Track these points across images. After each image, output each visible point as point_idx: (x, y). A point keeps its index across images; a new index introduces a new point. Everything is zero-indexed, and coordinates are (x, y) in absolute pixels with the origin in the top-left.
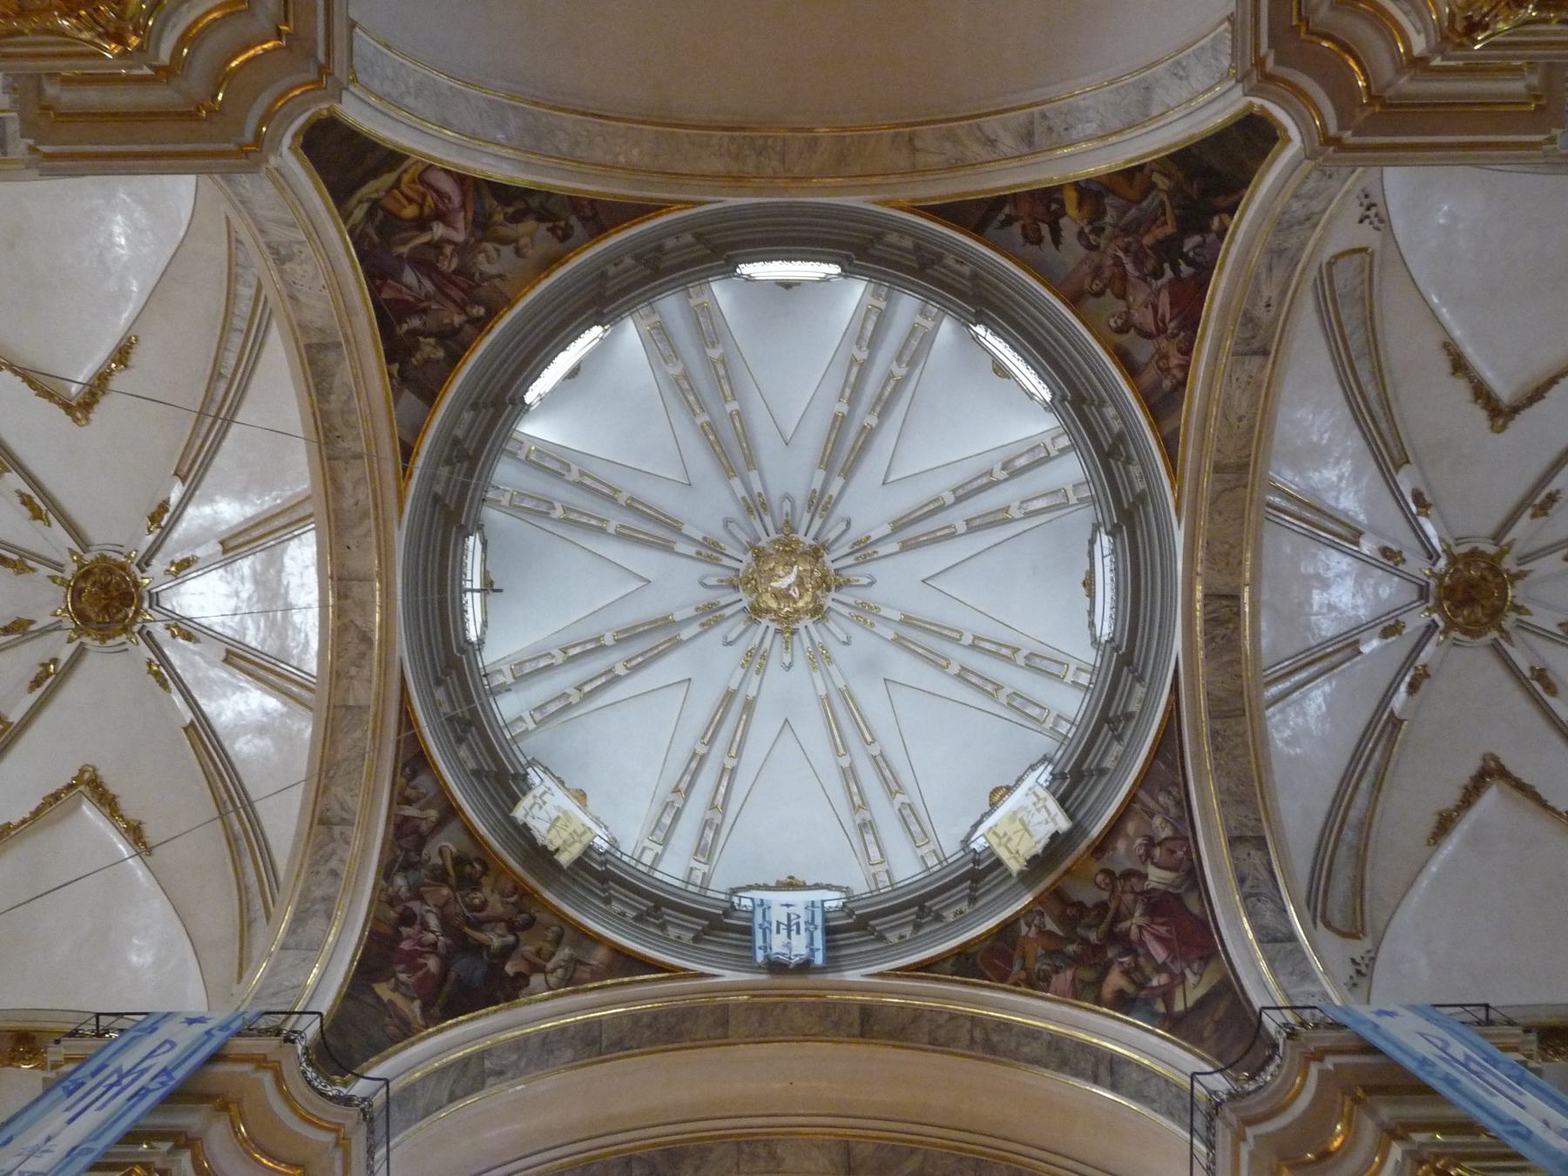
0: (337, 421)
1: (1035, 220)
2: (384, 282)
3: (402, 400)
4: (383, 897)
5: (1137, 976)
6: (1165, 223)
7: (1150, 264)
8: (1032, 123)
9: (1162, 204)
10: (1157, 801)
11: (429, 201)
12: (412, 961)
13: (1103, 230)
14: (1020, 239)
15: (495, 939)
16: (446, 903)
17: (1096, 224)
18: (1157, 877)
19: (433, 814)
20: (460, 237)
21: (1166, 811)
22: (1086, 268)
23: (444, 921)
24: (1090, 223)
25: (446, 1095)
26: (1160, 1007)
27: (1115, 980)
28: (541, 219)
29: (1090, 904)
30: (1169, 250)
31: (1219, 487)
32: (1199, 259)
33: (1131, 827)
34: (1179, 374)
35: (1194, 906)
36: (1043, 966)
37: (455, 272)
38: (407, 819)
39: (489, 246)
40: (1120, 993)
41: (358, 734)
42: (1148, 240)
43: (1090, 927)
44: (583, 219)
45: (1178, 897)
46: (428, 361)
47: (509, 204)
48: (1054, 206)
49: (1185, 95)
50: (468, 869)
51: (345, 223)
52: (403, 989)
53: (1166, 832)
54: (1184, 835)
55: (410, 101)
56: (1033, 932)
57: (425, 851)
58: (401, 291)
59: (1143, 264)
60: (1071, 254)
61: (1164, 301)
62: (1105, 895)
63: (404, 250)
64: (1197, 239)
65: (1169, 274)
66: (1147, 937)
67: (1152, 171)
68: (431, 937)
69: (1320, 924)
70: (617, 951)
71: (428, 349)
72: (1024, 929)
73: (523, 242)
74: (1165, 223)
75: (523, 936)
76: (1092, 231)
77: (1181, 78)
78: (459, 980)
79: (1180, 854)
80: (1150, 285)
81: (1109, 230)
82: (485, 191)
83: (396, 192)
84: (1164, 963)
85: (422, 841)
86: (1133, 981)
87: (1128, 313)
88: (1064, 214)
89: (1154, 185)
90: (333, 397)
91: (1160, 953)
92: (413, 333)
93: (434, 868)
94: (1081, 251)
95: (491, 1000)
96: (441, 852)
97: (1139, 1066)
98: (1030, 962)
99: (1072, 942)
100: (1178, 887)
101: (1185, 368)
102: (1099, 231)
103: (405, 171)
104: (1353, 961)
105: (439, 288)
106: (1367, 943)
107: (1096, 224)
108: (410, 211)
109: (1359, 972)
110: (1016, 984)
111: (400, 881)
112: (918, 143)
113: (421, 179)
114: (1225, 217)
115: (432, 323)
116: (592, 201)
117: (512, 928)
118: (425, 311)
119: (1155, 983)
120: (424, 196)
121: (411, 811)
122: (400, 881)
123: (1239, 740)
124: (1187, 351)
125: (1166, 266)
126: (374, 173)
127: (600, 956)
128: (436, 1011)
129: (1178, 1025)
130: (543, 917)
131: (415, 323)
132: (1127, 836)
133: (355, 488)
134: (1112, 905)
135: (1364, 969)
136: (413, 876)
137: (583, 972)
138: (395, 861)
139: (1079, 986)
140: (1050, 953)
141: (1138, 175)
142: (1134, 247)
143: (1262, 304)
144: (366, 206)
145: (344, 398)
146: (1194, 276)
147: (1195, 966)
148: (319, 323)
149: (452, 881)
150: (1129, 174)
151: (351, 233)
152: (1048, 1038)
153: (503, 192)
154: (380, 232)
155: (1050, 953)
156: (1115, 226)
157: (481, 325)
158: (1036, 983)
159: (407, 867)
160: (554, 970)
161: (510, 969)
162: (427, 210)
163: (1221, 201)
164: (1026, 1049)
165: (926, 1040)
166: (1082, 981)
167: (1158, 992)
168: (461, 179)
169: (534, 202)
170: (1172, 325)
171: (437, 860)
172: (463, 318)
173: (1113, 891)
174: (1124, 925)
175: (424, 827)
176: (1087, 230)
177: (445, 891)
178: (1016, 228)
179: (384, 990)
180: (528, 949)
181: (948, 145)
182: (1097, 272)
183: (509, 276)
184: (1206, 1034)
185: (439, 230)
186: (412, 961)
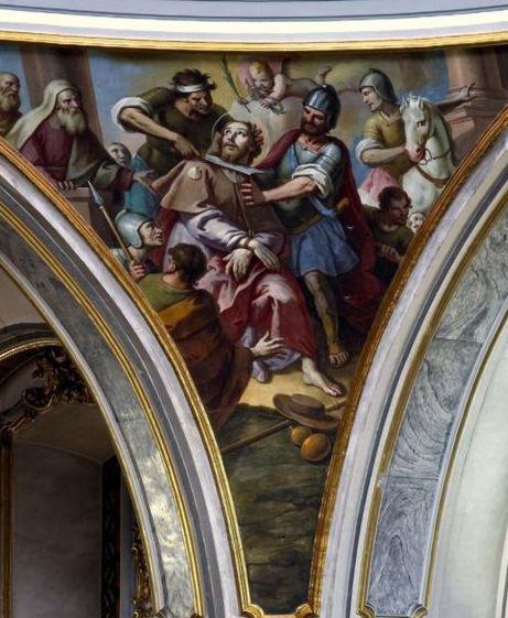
4: (137, 271)
12: (253, 314)
15: (310, 173)
16: (210, 185)
19: (56, 90)
23: (232, 213)
50: (181, 106)
52: (280, 363)
57: (110, 149)
68: (239, 256)
78: (321, 277)
85: (88, 140)
93: (145, 153)
96: (129, 126)
121: (30, 122)
122: (130, 226)
128: (336, 354)
130: (338, 76)
136: (134, 198)
149: (184, 146)
159: (116, 195)
160: (422, 151)
161: (368, 198)
171: (136, 142)
175: (70, 121)
177: (191, 170)
179: (258, 394)
180: (364, 148)
186: (253, 314)
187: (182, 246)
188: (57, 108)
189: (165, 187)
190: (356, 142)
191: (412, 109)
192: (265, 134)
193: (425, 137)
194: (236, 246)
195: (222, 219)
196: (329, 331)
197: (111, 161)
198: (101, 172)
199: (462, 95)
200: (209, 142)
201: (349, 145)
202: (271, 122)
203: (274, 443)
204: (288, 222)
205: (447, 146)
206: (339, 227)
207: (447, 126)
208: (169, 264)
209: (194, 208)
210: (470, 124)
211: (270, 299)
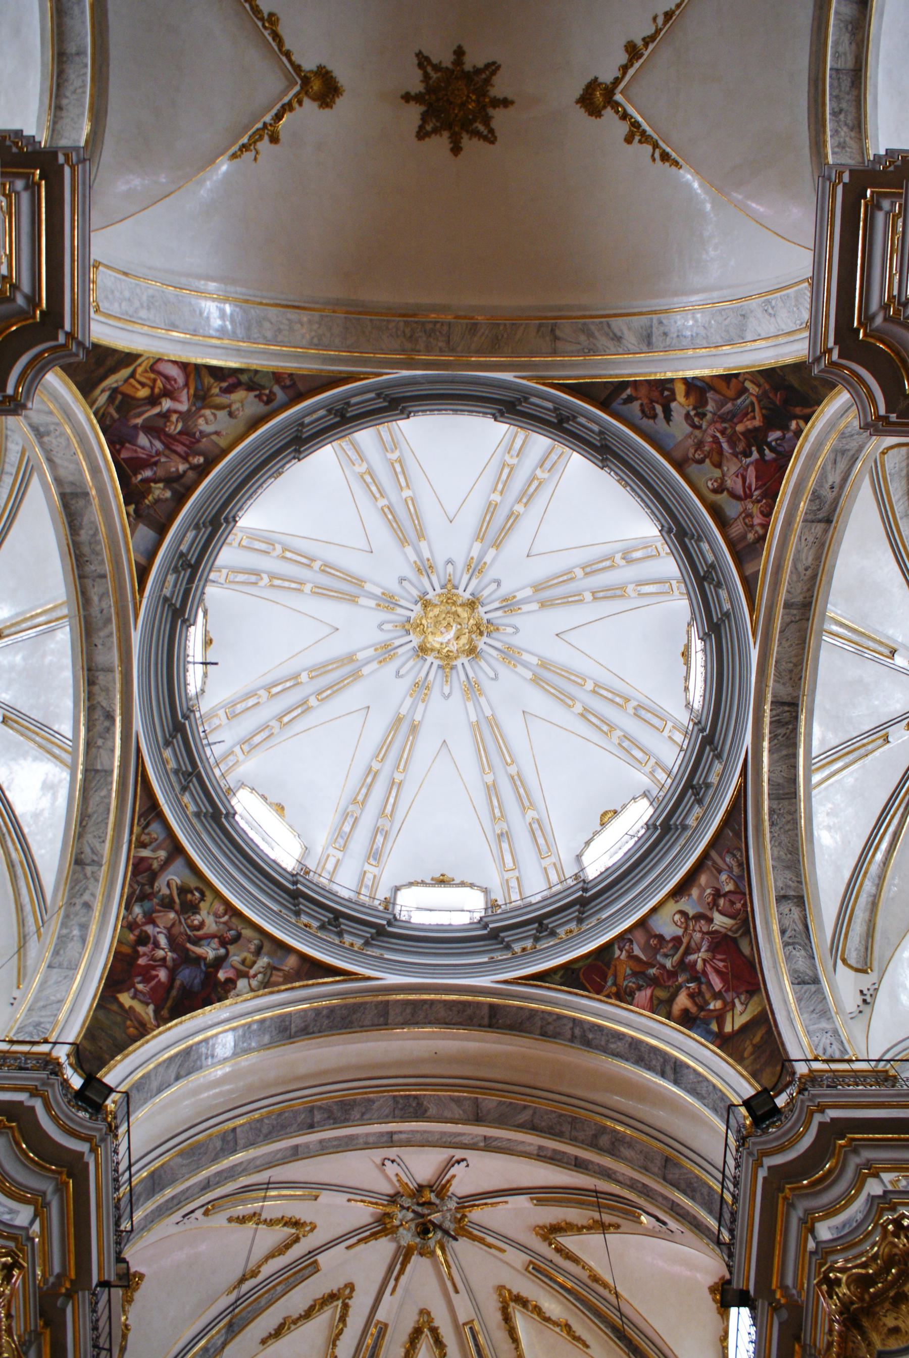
0: (86, 550)
1: (652, 401)
2: (123, 446)
3: (138, 533)
4: (125, 924)
5: (699, 1000)
6: (754, 418)
7: (740, 447)
8: (651, 327)
9: (752, 404)
10: (724, 861)
11: (159, 384)
12: (147, 974)
13: (704, 415)
14: (639, 414)
15: (209, 951)
16: (173, 925)
17: (700, 410)
18: (720, 921)
19: (162, 854)
20: (183, 407)
21: (731, 869)
22: (690, 441)
23: (171, 939)
24: (695, 408)
25: (173, 1077)
26: (714, 1027)
27: (682, 1001)
28: (250, 388)
29: (668, 938)
30: (756, 438)
31: (788, 620)
32: (780, 449)
33: (703, 879)
34: (761, 532)
35: (746, 950)
37: (180, 433)
38: (142, 859)
39: (207, 412)
40: (685, 1011)
41: (103, 793)
42: (740, 428)
43: (666, 956)
44: (284, 388)
45: (734, 940)
46: (157, 501)
47: (224, 380)
48: (666, 393)
49: (773, 331)
50: (189, 896)
51: (91, 407)
52: (141, 997)
53: (729, 887)
54: (743, 891)
55: (143, 314)
56: (624, 956)
57: (156, 885)
58: (136, 451)
59: (735, 445)
60: (678, 429)
61: (751, 474)
62: (680, 932)
63: (139, 421)
64: (778, 434)
65: (755, 455)
66: (709, 969)
67: (745, 380)
68: (161, 953)
69: (839, 962)
70: (304, 958)
71: (157, 492)
72: (617, 952)
73: (234, 407)
74: (754, 418)
75: (231, 948)
76: (697, 415)
77: (770, 315)
78: (182, 984)
79: (738, 906)
80: (741, 462)
81: (709, 416)
82: (204, 372)
83: (132, 381)
84: (720, 991)
85: (154, 876)
86: (695, 1004)
87: (723, 479)
88: (674, 400)
89: (745, 390)
90: (82, 532)
91: (718, 984)
92: (146, 481)
94: (689, 429)
95: (209, 1002)
96: (168, 885)
97: (695, 1071)
98: (620, 980)
99: (653, 966)
100: (736, 932)
101: (765, 526)
102: (702, 416)
103: (140, 365)
104: (861, 992)
105: (167, 446)
106: (873, 977)
107: (700, 410)
108: (143, 393)
109: (865, 1001)
110: (608, 996)
111: (137, 910)
112: (558, 333)
113: (152, 369)
114: (801, 423)
115: (161, 472)
116: (291, 375)
117: (224, 943)
118: (156, 464)
119: (712, 1007)
120: (155, 381)
121: (145, 853)
122: (137, 910)
123: (790, 817)
124: (767, 514)
125: (754, 449)
126: (114, 370)
127: (291, 962)
128: (165, 1013)
129: (726, 1043)
130: (247, 932)
131: (148, 473)
132: (700, 885)
133: (100, 601)
134: (685, 940)
135: (868, 1000)
136: (147, 904)
137: (277, 977)
138: (135, 891)
139: (655, 1002)
140: (635, 974)
141: (734, 381)
142: (729, 431)
143: (827, 486)
144: (106, 395)
145: (91, 532)
146: (774, 460)
147: (743, 997)
148: (71, 478)
149: (177, 907)
150: (727, 378)
151: (95, 414)
152: (630, 1040)
153: (217, 372)
154: (118, 410)
155: (635, 974)
156: (714, 414)
157: (203, 471)
158: (624, 996)
159: (143, 898)
160: (255, 976)
161: (222, 975)
162: (157, 391)
163: (798, 410)
164: (613, 1046)
165: (538, 1032)
166: (658, 998)
167: (715, 1013)
168: (184, 366)
169: (244, 378)
170: (756, 493)
171: (165, 891)
172: (187, 466)
173: (686, 929)
174: (692, 957)
175: (155, 865)
176: (692, 413)
177: (172, 915)
178: (636, 405)
179: (125, 999)
180: (235, 959)
181: (582, 338)
182: (699, 445)
183: (224, 433)
184: (746, 1054)
185: (167, 404)
186: (147, 974)
187: (146, 932)
188: (157, 858)
189: (159, 911)
190: (234, 955)
191: (263, 961)
192: (206, 928)
193: (260, 973)
194: (163, 949)
195: (166, 937)
196: (169, 1004)
197: (152, 887)
198: (147, 887)
199: (287, 969)
200: (187, 913)
201: (231, 953)
202: (211, 926)
203: (119, 1019)
204: (186, 959)
205: (266, 980)
206: (203, 976)
207: (271, 975)
208: (137, 932)
209: (161, 926)
210: (281, 980)
211: (157, 976)
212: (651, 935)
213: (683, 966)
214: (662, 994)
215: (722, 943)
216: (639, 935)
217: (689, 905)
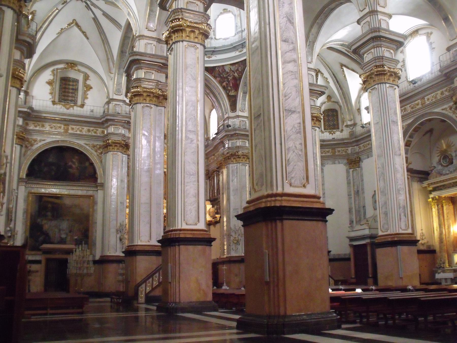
27: (224, 84)
33: (236, 65)
35: (238, 82)
36: (217, 75)
40: (224, 86)
53: (240, 70)
62: (229, 71)
91: (231, 85)
129: (229, 96)
155: (218, 74)
158: (215, 77)
174: (229, 77)
212: (224, 68)
213: (227, 78)
214: (222, 81)
215: (234, 78)
216: (221, 67)
217: (233, 68)
